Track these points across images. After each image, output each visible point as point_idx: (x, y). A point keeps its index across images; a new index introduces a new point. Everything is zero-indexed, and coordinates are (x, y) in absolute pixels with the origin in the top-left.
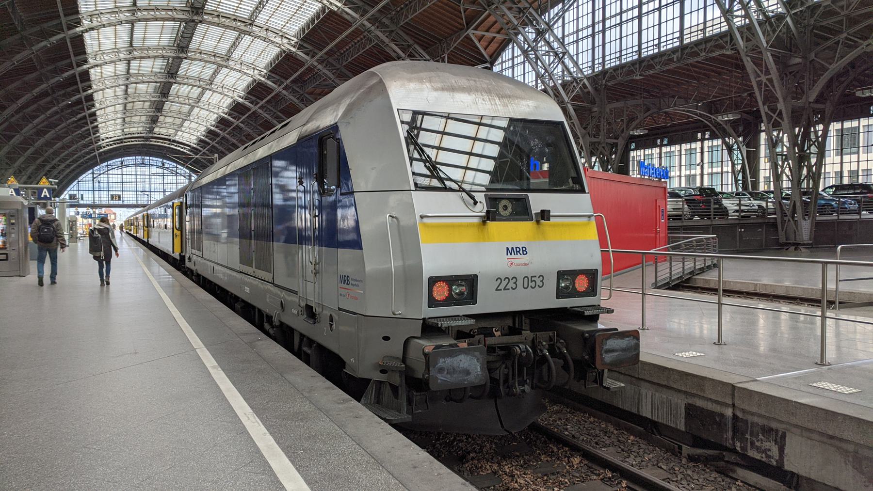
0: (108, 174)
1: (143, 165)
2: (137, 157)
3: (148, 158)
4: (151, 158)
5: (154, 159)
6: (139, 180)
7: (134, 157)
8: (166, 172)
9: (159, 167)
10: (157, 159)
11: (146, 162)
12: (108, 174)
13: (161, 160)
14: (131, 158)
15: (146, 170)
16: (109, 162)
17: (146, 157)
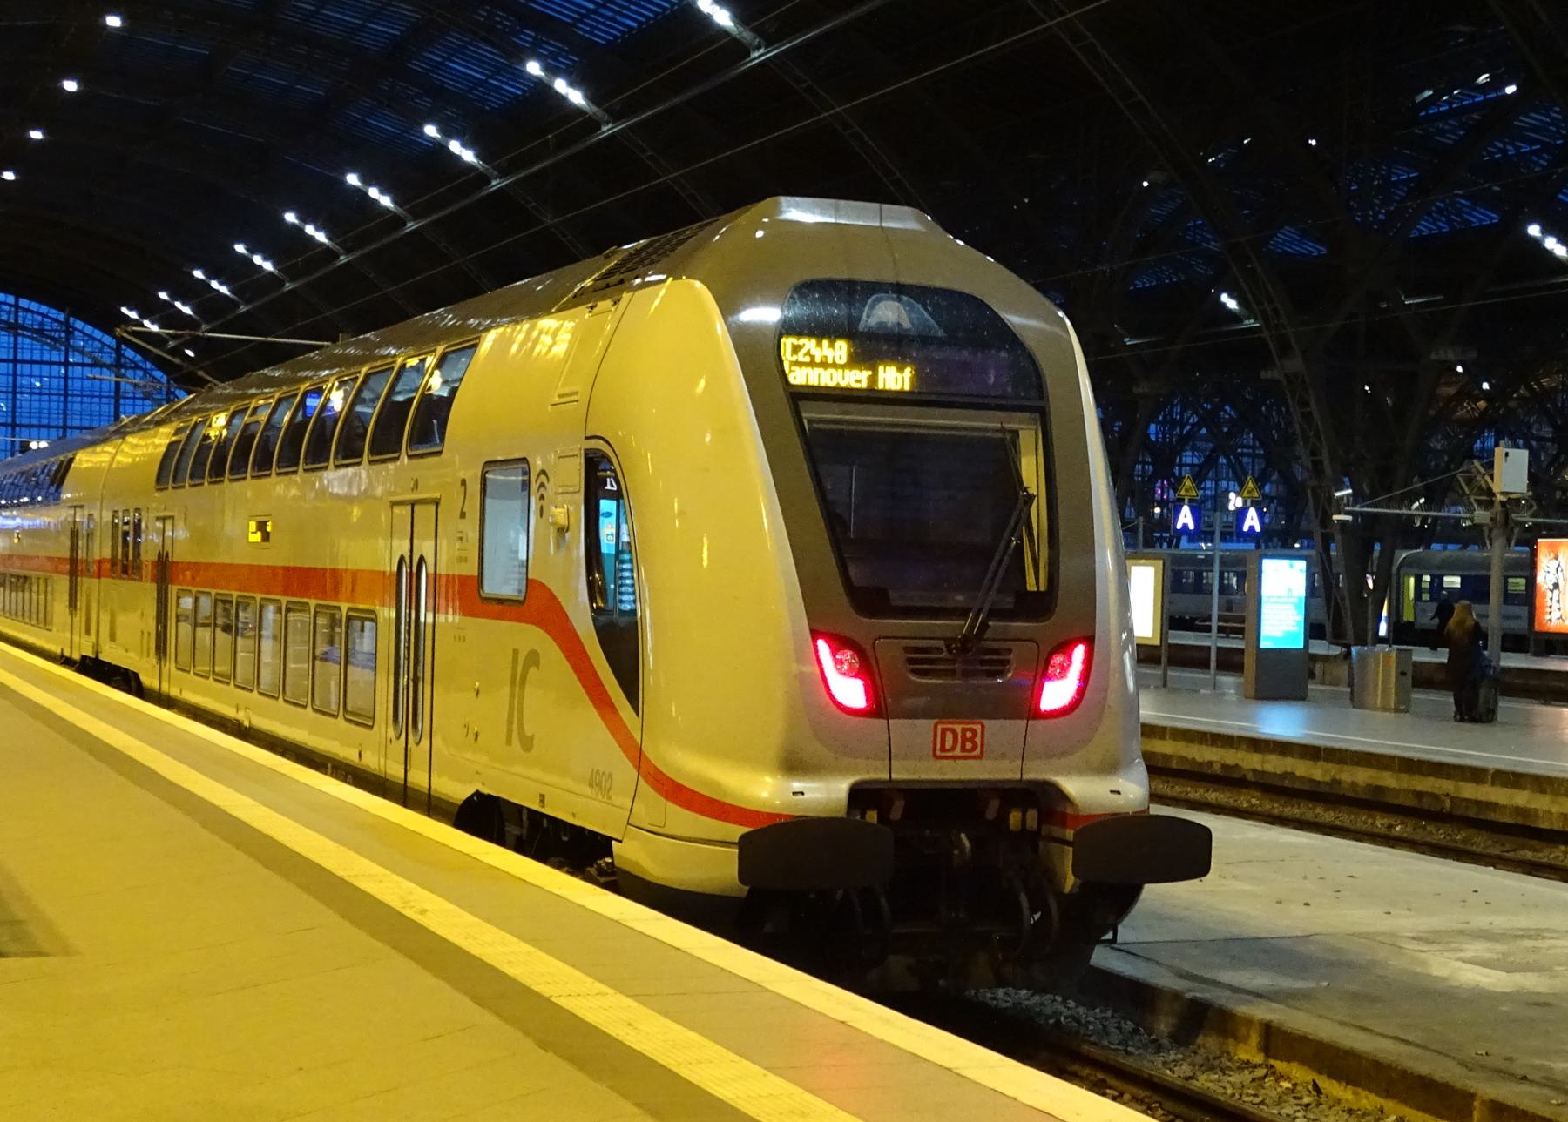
8: (29, 348)
13: (11, 299)
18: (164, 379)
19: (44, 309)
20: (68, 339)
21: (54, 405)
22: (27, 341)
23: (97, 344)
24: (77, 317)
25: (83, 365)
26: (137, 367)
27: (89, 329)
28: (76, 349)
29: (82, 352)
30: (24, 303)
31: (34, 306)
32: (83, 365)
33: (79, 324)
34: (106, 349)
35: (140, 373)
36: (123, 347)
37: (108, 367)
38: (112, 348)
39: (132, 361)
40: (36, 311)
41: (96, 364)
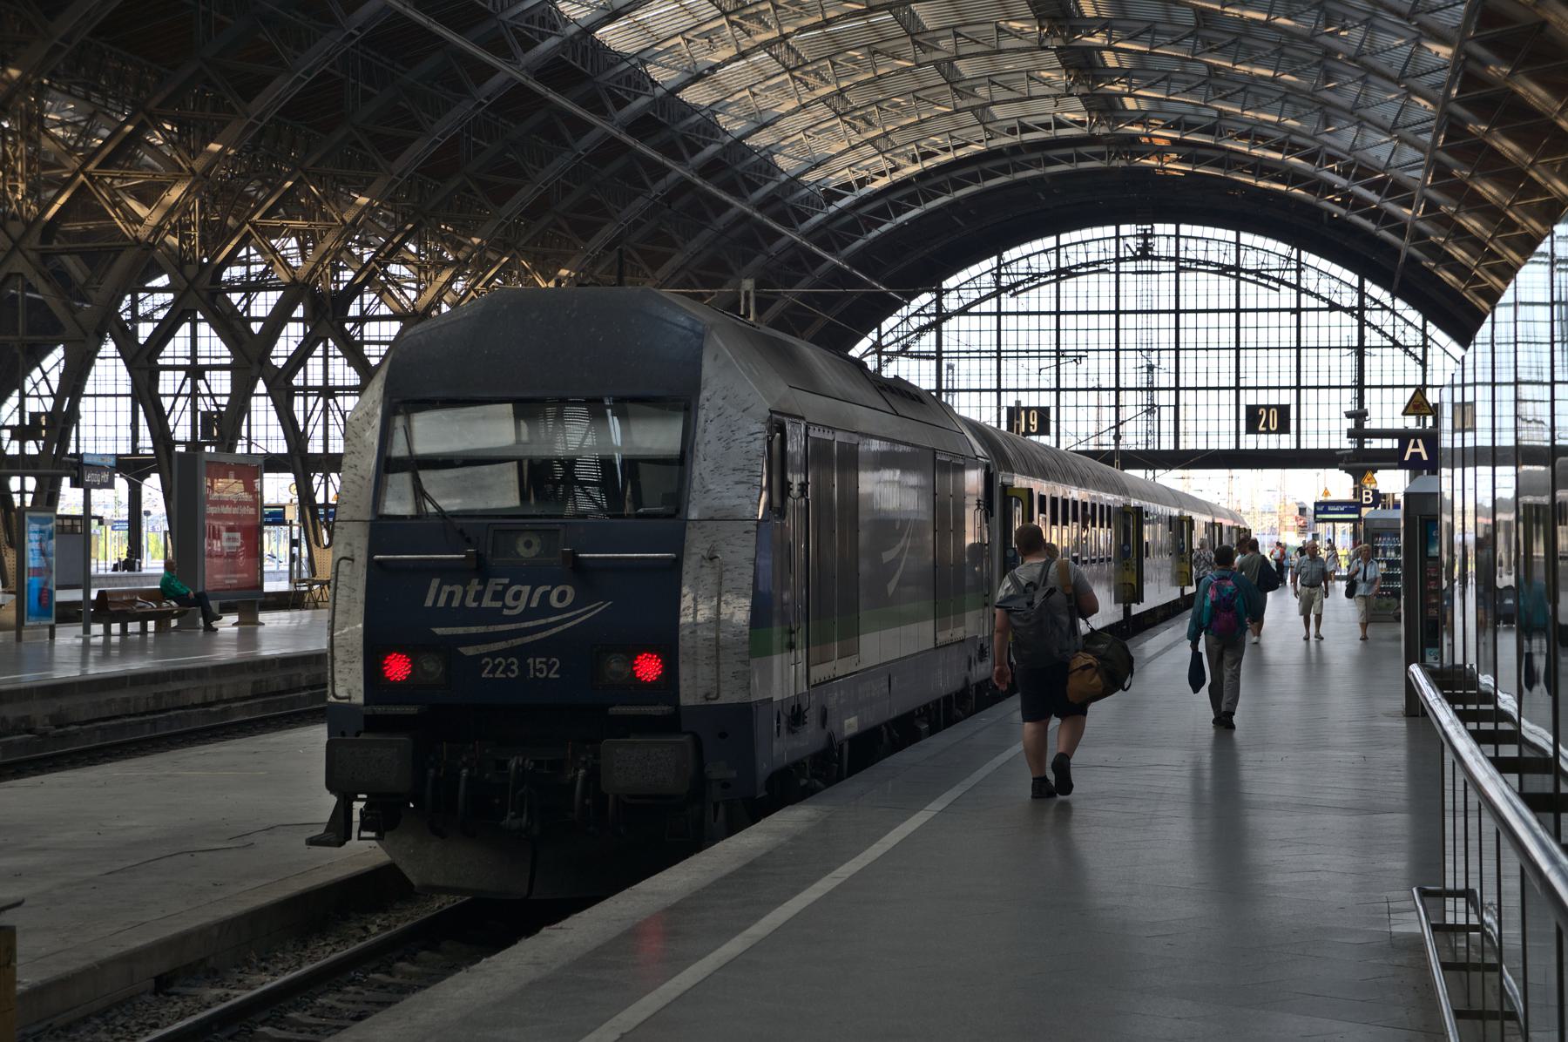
0: (999, 314)
1: (1145, 265)
2: (1126, 229)
3: (1170, 229)
4: (1185, 229)
5: (1197, 230)
6: (1128, 339)
7: (1110, 230)
8: (1252, 295)
9: (1223, 270)
10: (1209, 231)
11: (1162, 246)
12: (999, 314)
13: (1231, 235)
14: (1098, 232)
15: (1160, 289)
16: (1008, 256)
17: (1159, 228)
18: (1418, 321)
19: (1271, 244)
20: (1299, 278)
21: (1285, 362)
22: (1252, 286)
23: (1334, 284)
24: (1310, 251)
25: (1318, 309)
26: (1384, 308)
27: (1325, 264)
28: (1307, 292)
29: (1318, 296)
30: (1246, 238)
31: (1259, 241)
32: (1318, 309)
33: (1309, 258)
34: (1345, 289)
35: (1386, 313)
36: (1367, 284)
37: (1349, 310)
38: (1352, 287)
39: (1377, 302)
40: (1265, 250)
41: (1333, 307)
